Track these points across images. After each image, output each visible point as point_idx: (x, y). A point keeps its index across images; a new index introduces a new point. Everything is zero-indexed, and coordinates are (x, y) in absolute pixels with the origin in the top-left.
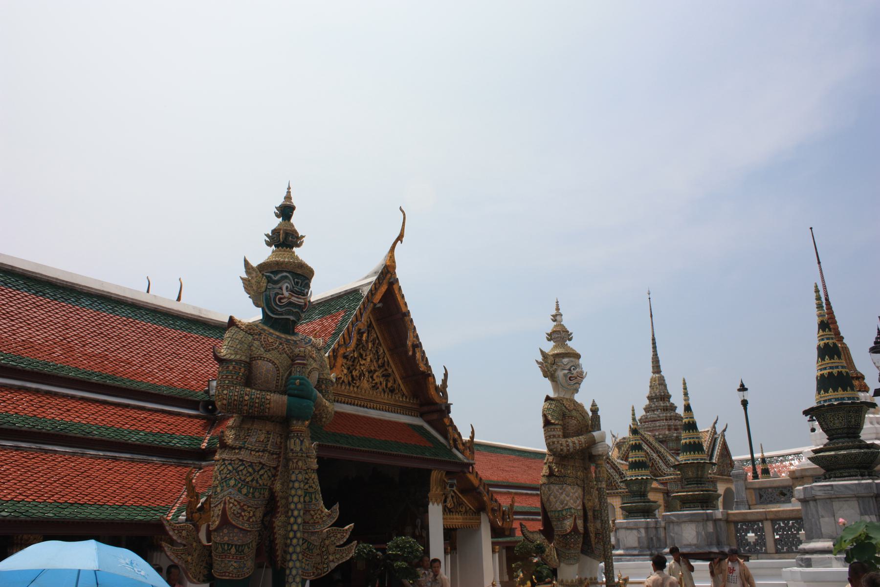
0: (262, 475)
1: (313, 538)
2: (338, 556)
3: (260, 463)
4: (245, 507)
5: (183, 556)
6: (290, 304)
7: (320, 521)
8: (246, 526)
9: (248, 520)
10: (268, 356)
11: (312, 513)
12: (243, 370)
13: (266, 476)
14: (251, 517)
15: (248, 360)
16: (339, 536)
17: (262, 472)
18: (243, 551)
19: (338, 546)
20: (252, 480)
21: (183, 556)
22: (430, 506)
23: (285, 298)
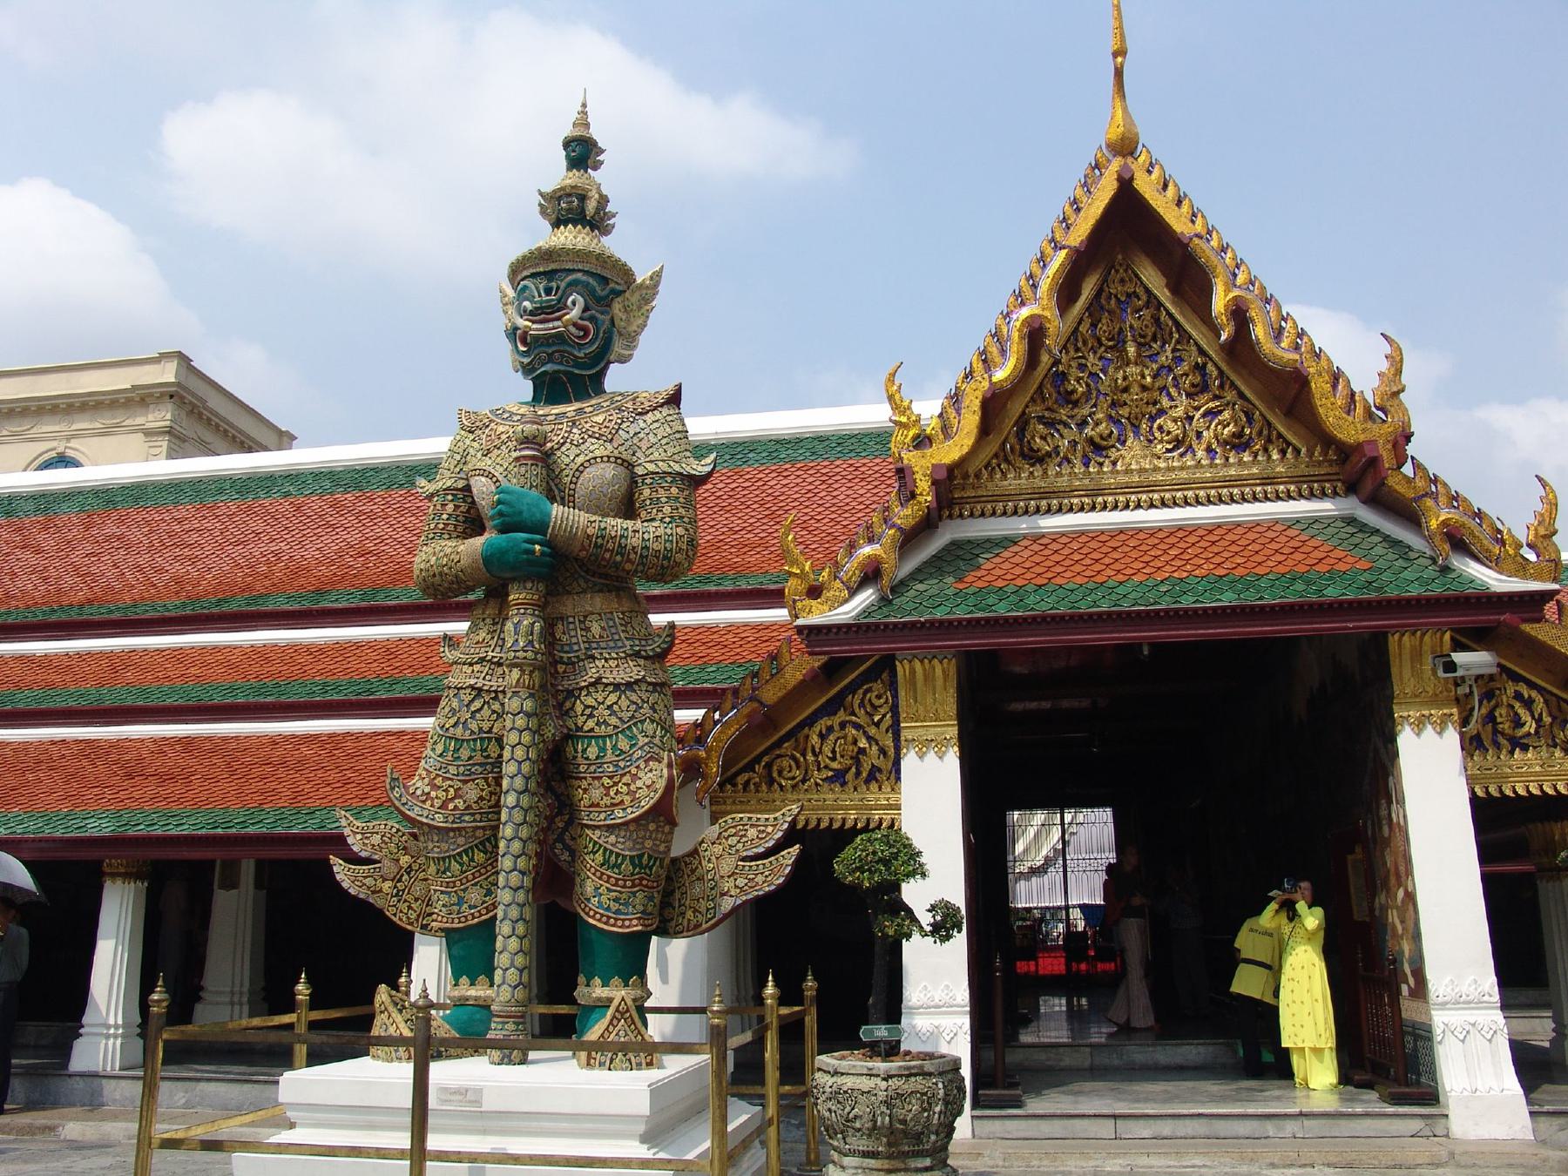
0: (479, 710)
1: (612, 839)
2: (741, 882)
3: (472, 687)
4: (438, 781)
5: (367, 881)
6: (536, 338)
7: (627, 799)
8: (439, 820)
9: (444, 806)
10: (486, 463)
11: (606, 781)
12: (450, 507)
13: (486, 712)
14: (452, 799)
15: (461, 484)
16: (752, 833)
17: (477, 704)
18: (448, 869)
19: (744, 859)
20: (455, 725)
21: (367, 881)
22: (1406, 740)
23: (525, 333)
